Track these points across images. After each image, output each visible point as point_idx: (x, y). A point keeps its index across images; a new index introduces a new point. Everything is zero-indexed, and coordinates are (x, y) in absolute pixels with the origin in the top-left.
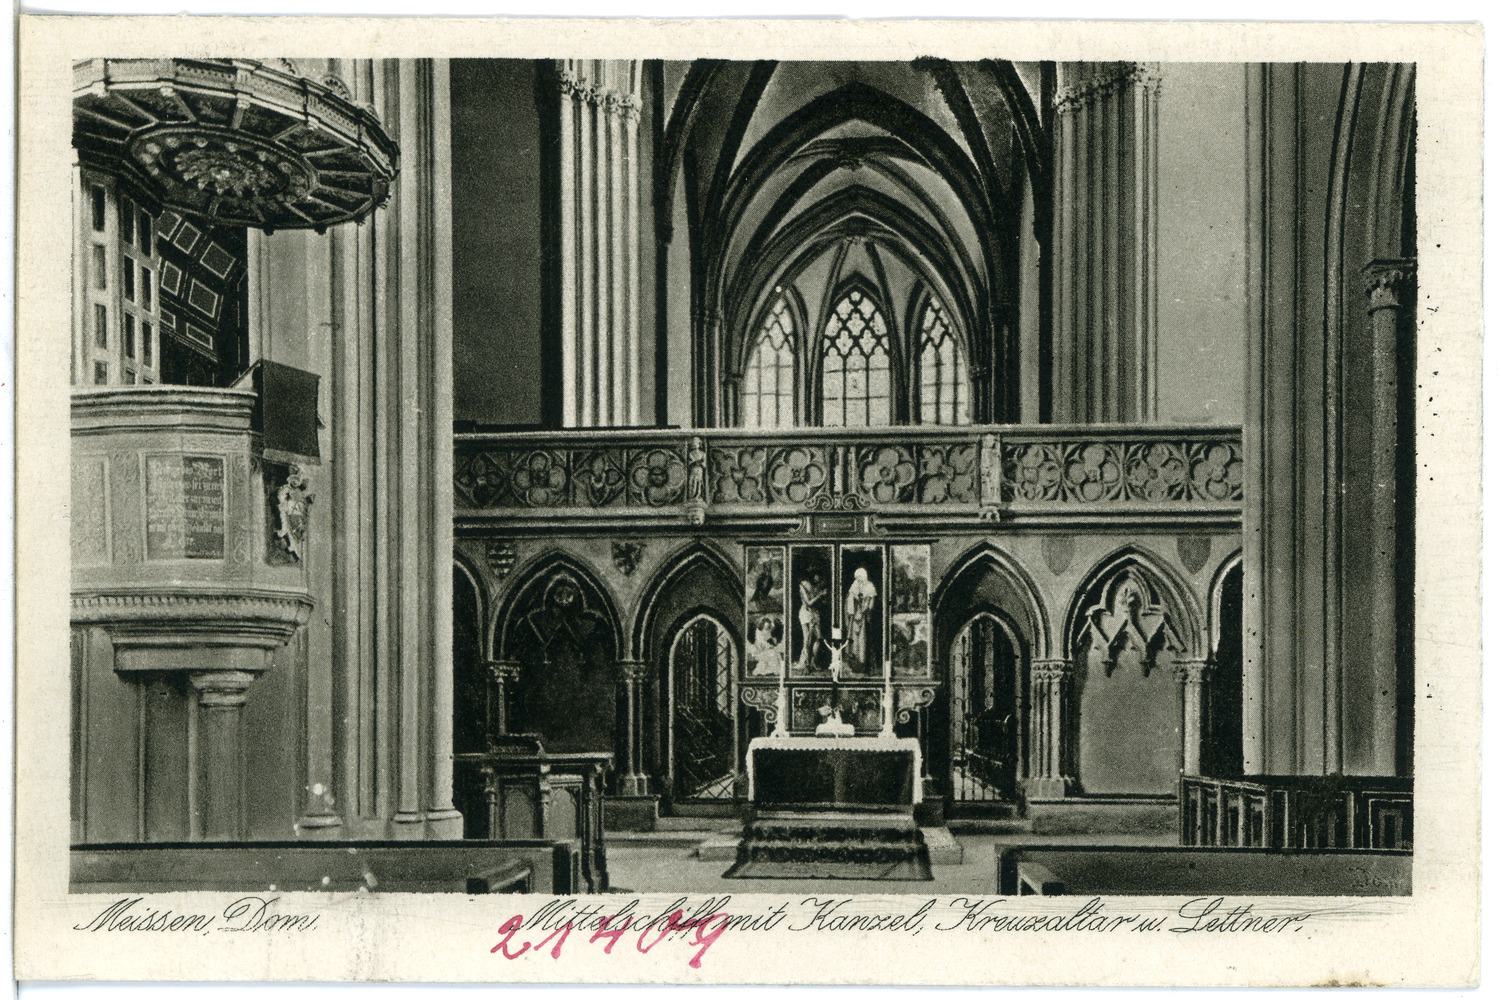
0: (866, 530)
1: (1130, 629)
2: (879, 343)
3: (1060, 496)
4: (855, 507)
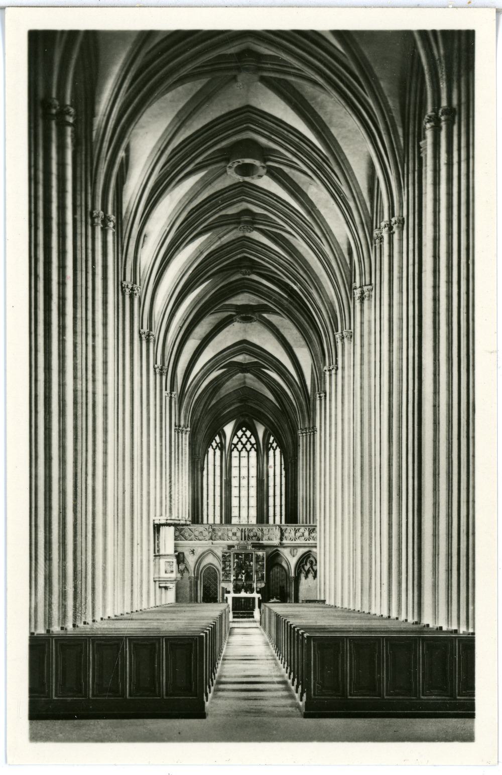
1: (310, 569)
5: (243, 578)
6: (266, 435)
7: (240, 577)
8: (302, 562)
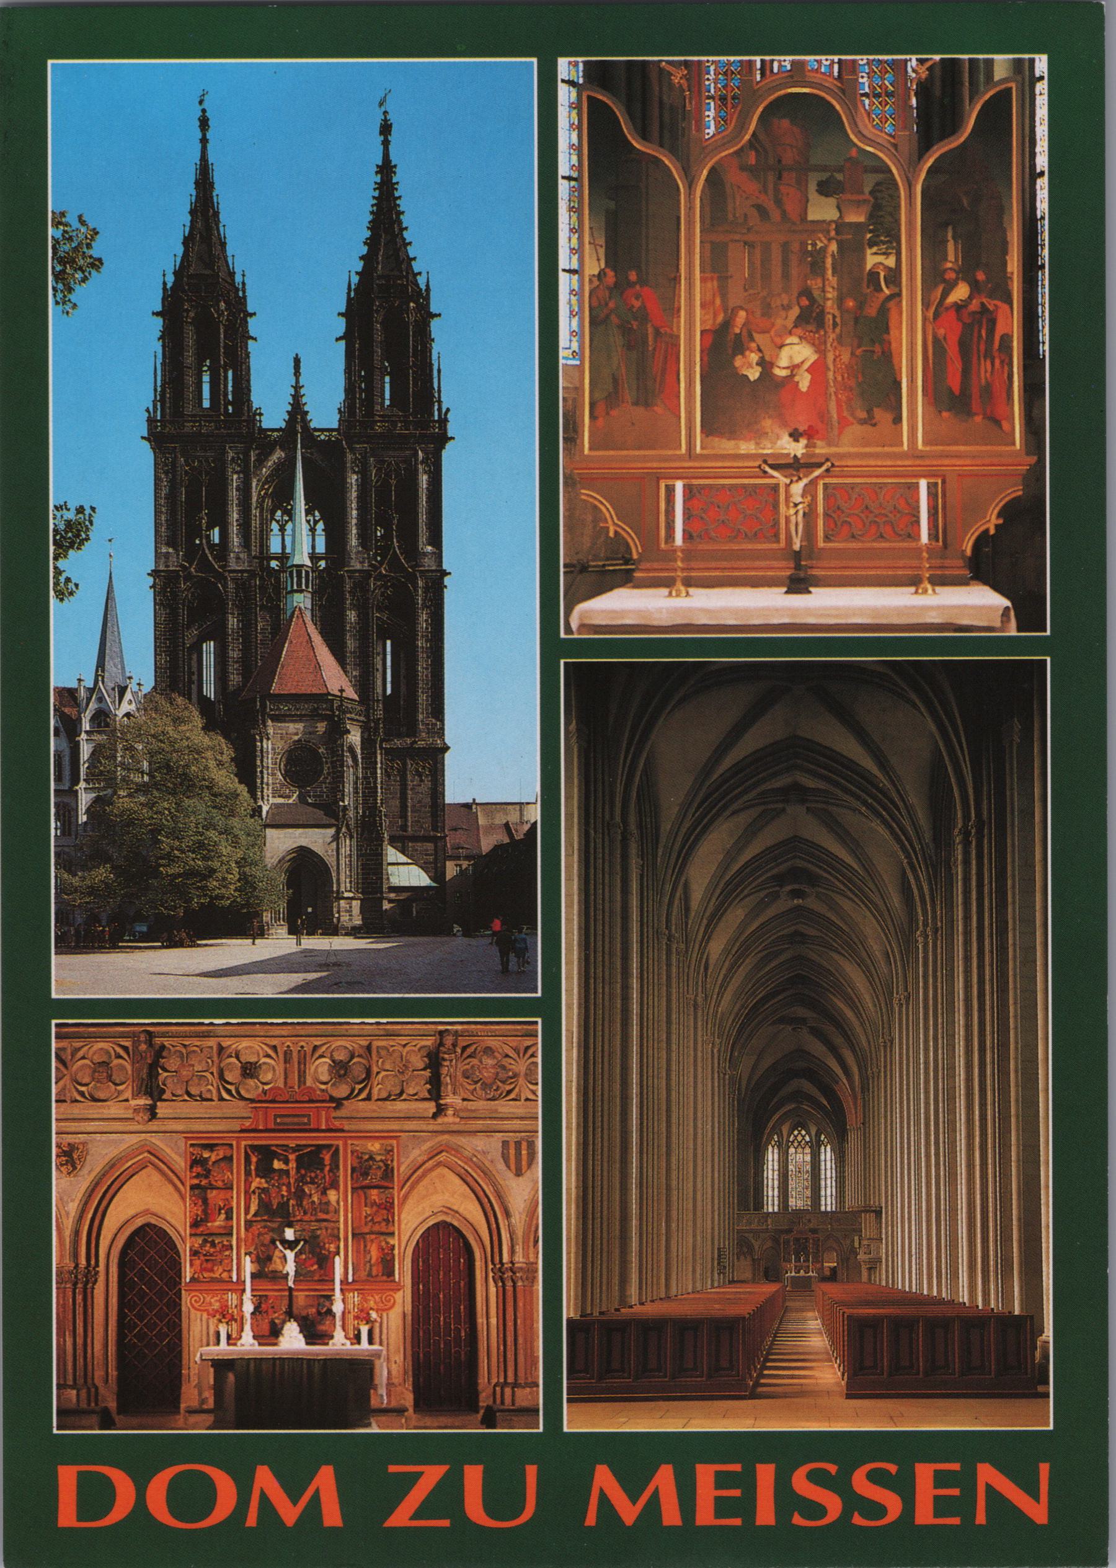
7: (276, 1264)
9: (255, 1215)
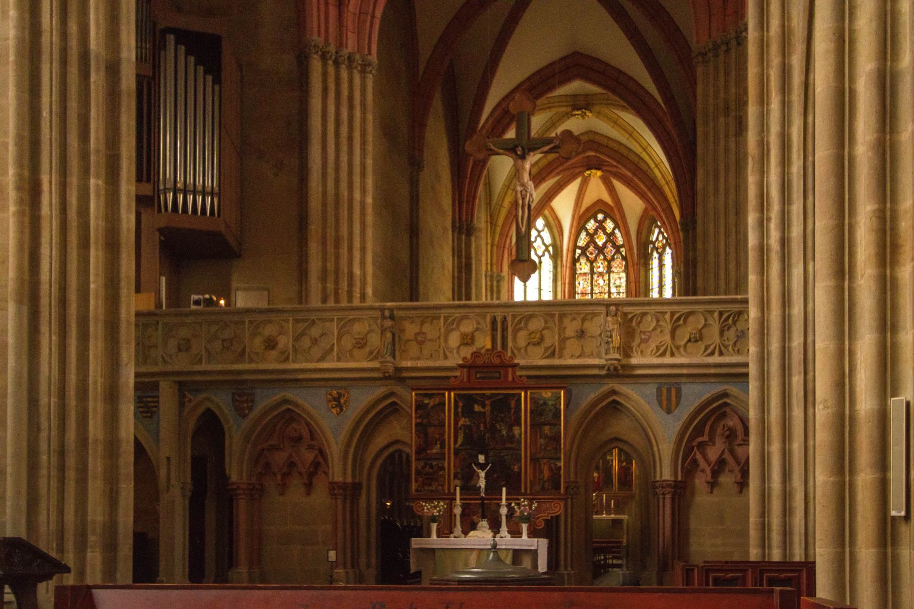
0: (510, 379)
1: (727, 455)
2: (618, 251)
3: (668, 353)
4: (501, 360)
5: (482, 483)
6: (647, 222)
8: (699, 431)
9: (461, 445)
